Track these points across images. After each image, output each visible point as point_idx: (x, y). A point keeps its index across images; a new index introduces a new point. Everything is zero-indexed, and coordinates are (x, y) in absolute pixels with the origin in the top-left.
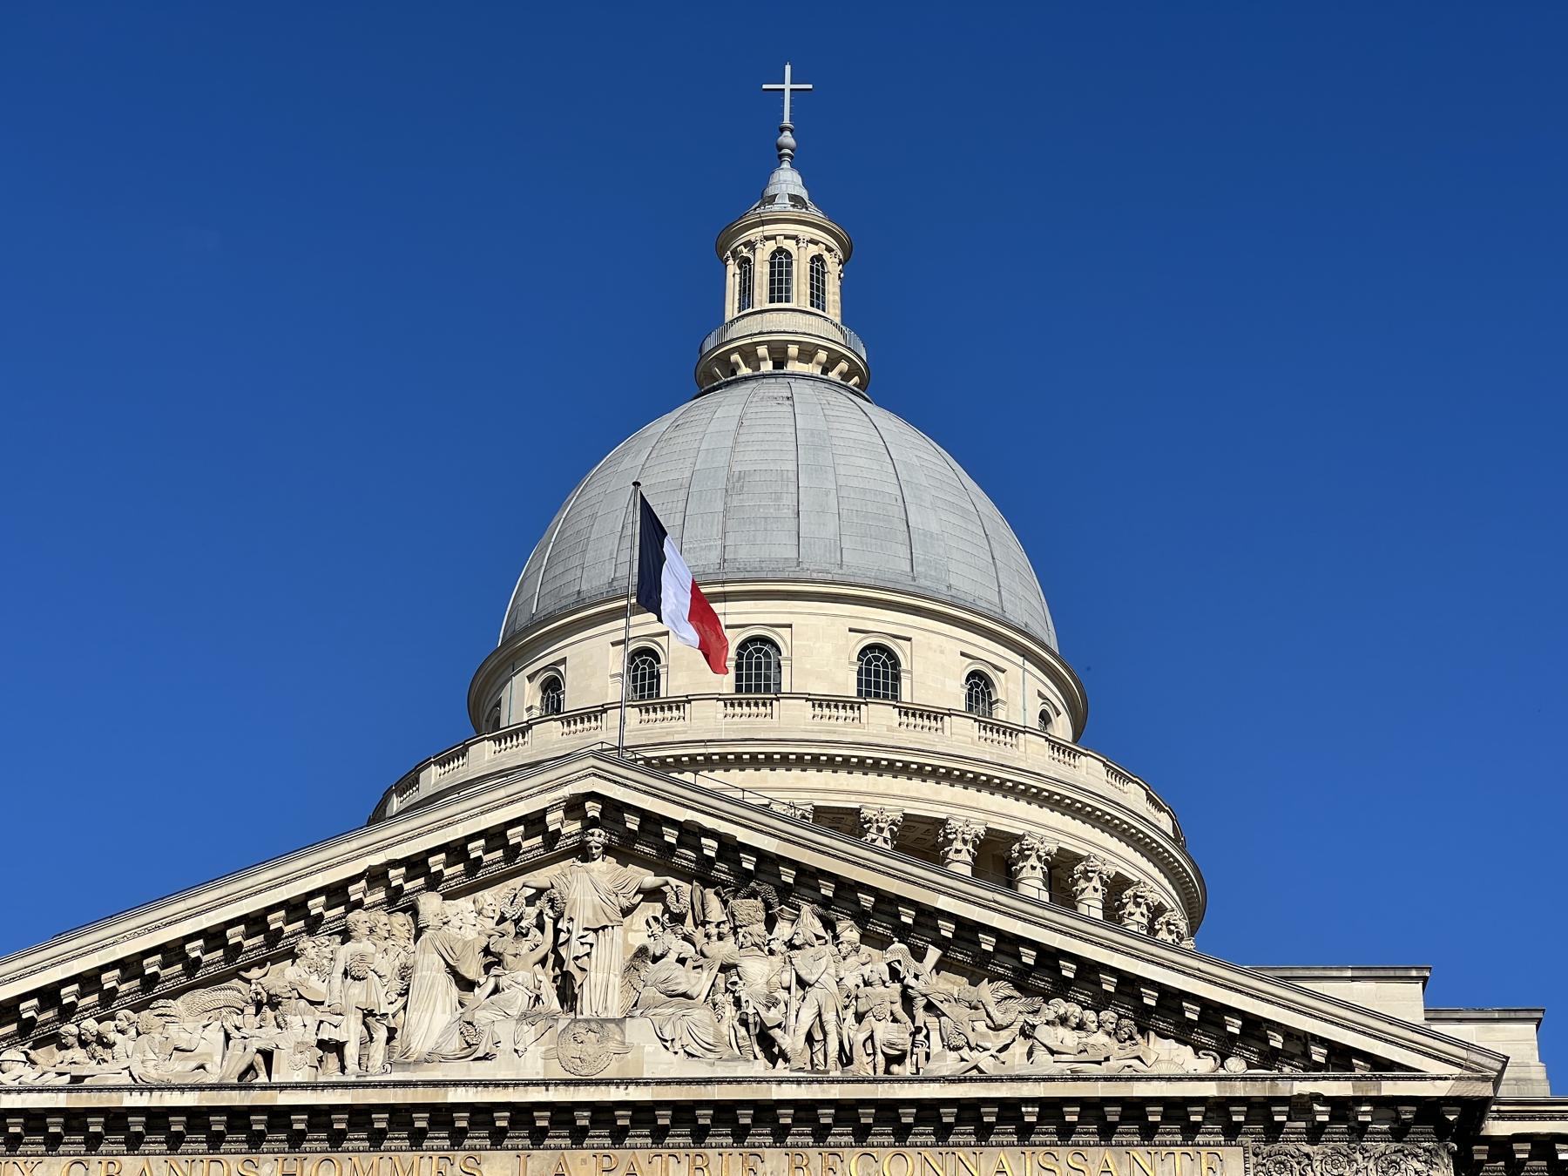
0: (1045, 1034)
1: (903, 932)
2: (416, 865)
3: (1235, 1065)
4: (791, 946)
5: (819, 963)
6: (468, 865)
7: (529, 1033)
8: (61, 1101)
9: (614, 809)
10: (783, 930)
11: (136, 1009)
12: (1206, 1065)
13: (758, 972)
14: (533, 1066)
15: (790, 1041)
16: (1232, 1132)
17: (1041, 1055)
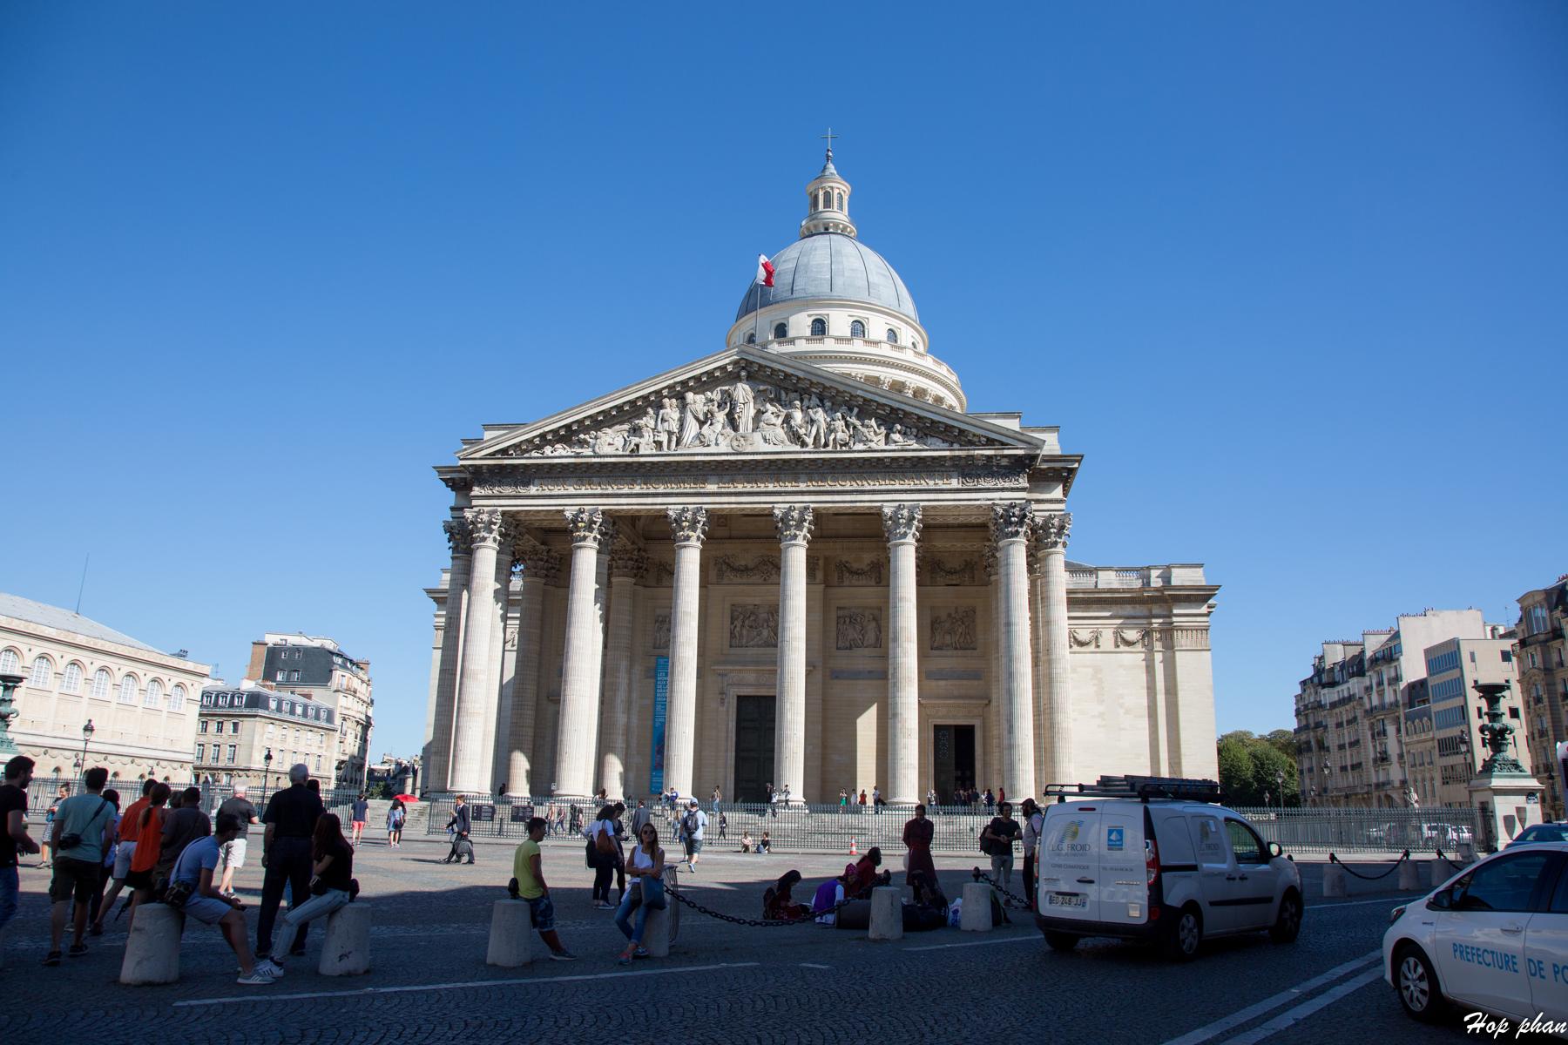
1: (846, 403)
2: (684, 383)
5: (820, 415)
6: (703, 383)
10: (806, 403)
12: (946, 446)
13: (798, 416)
14: (723, 448)
15: (810, 441)
16: (955, 466)
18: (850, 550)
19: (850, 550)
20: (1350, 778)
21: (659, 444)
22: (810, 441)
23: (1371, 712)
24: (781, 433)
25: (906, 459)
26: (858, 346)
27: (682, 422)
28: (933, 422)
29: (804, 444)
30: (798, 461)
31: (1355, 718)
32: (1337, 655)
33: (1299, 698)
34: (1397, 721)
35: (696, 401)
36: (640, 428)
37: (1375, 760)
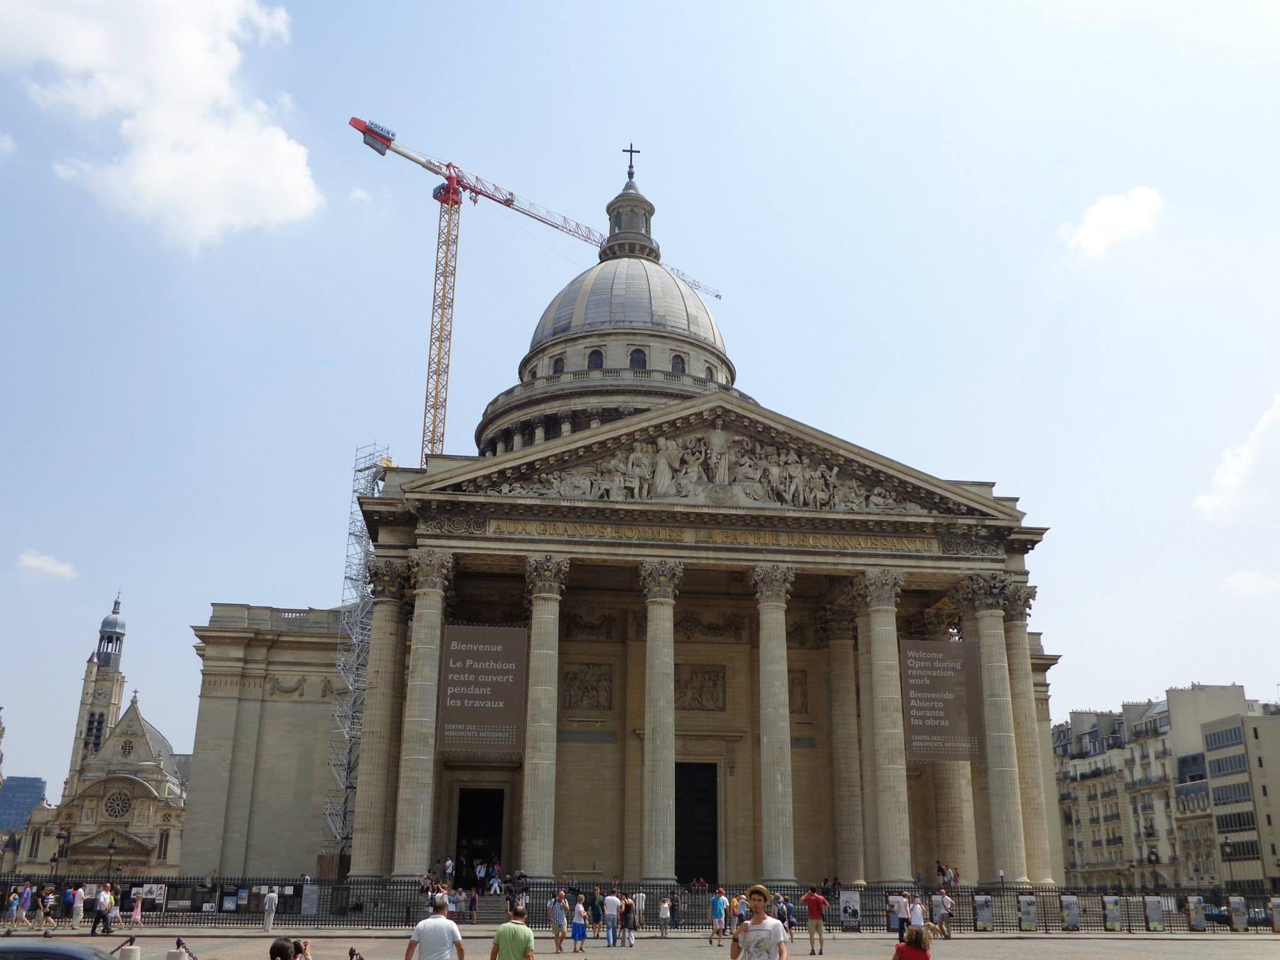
0: (873, 499)
1: (826, 461)
2: (658, 427)
3: (935, 512)
4: (786, 463)
5: (795, 471)
7: (700, 489)
8: (538, 502)
9: (727, 411)
10: (783, 458)
11: (561, 470)
12: (925, 512)
13: (775, 471)
14: (701, 499)
15: (788, 497)
16: (936, 533)
17: (872, 505)
20: (1106, 853)
23: (1132, 786)
25: (889, 523)
28: (914, 487)
30: (781, 519)
31: (1115, 791)
34: (1166, 796)
36: (610, 472)
37: (1138, 835)
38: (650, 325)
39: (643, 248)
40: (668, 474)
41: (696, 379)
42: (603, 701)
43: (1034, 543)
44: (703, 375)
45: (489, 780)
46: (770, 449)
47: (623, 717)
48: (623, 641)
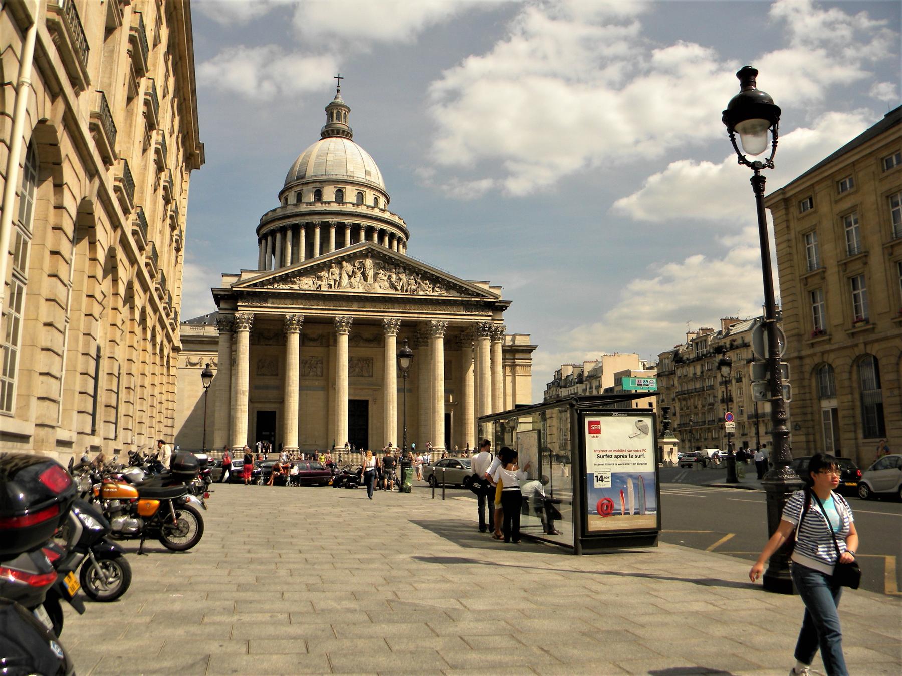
5: (403, 277)
6: (350, 259)
9: (373, 250)
12: (458, 295)
13: (394, 276)
14: (361, 290)
15: (399, 288)
18: (415, 337)
19: (415, 337)
21: (330, 286)
22: (399, 288)
24: (387, 284)
26: (363, 210)
27: (341, 275)
29: (397, 290)
32: (569, 371)
33: (546, 392)
35: (348, 267)
38: (345, 178)
39: (344, 132)
40: (347, 278)
41: (368, 207)
42: (319, 373)
43: (506, 307)
44: (372, 205)
45: (268, 407)
46: (392, 267)
47: (327, 379)
48: (328, 346)
